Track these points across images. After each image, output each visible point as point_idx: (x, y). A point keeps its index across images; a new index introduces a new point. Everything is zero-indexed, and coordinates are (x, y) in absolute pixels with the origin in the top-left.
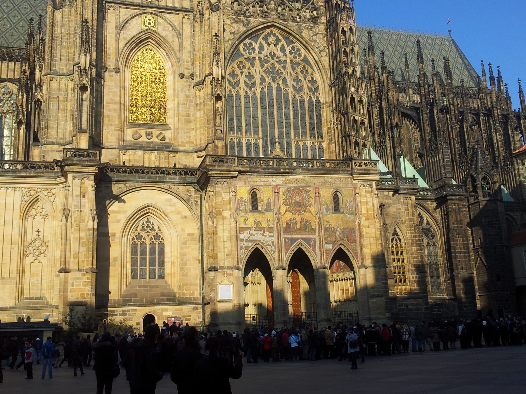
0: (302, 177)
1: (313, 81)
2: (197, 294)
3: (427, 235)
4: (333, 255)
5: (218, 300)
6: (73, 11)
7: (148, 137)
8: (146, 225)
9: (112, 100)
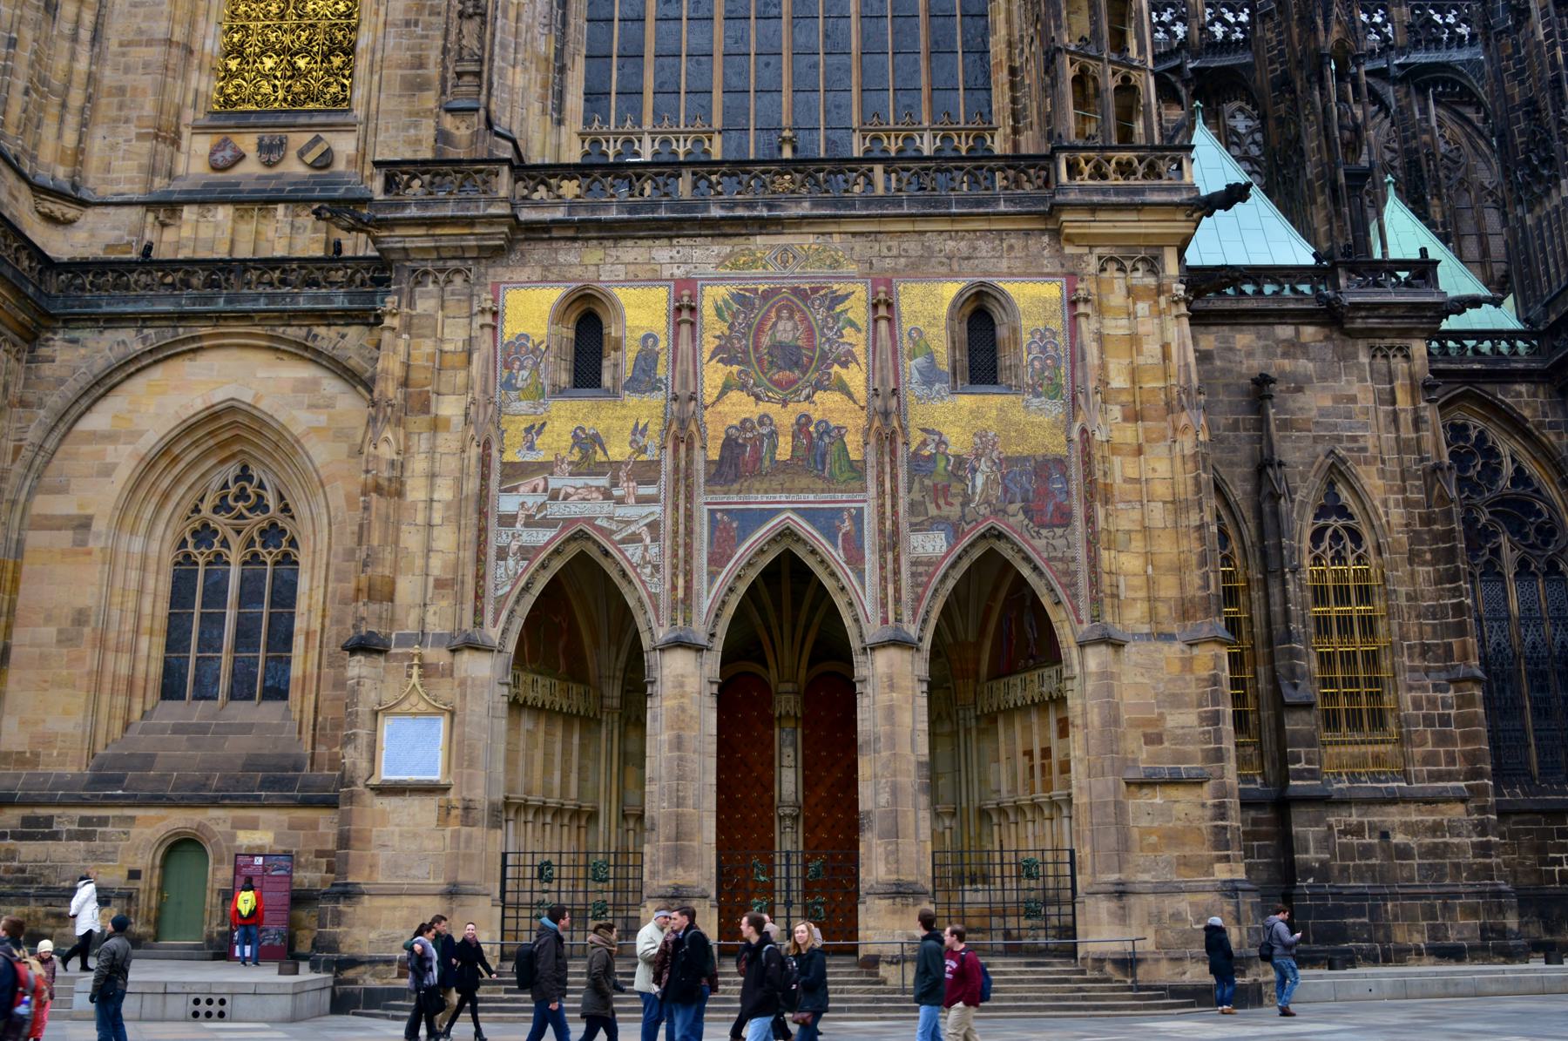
3: (1517, 531)
4: (951, 584)
5: (374, 781)
7: (265, 157)
8: (234, 489)
9: (140, 32)
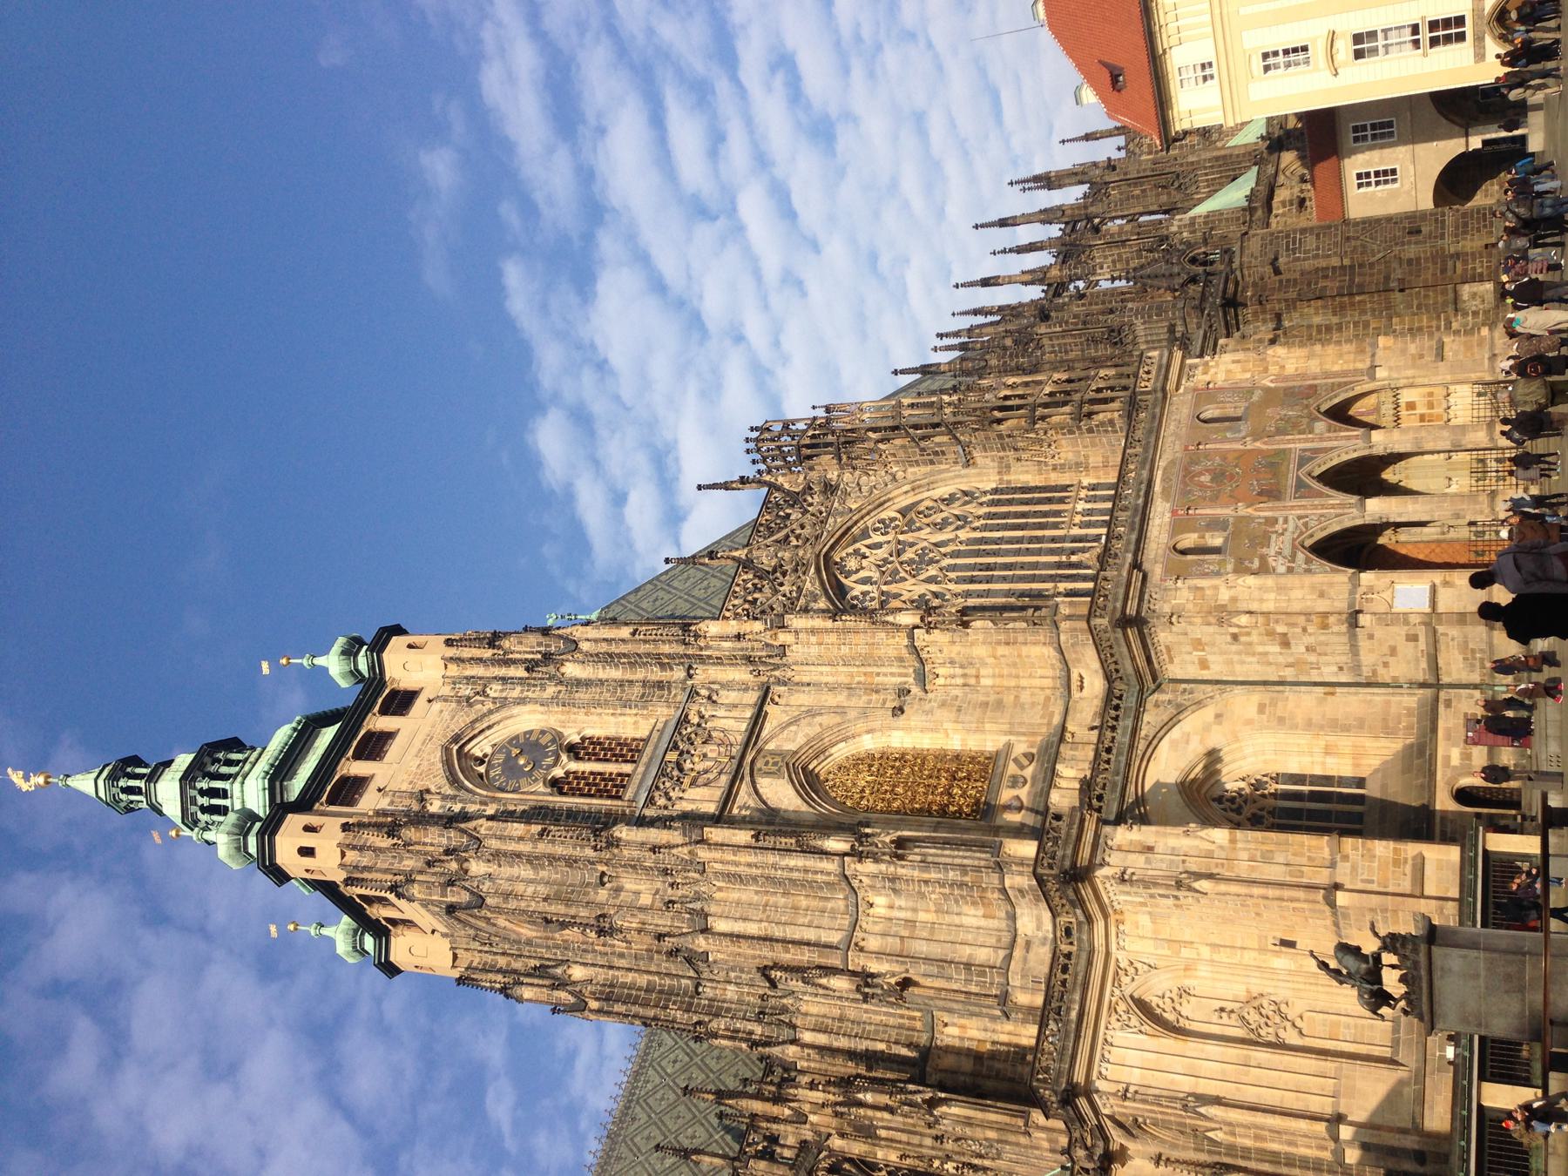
0: (1160, 473)
1: (949, 500)
2: (1411, 700)
5: (1428, 610)
6: (718, 895)
